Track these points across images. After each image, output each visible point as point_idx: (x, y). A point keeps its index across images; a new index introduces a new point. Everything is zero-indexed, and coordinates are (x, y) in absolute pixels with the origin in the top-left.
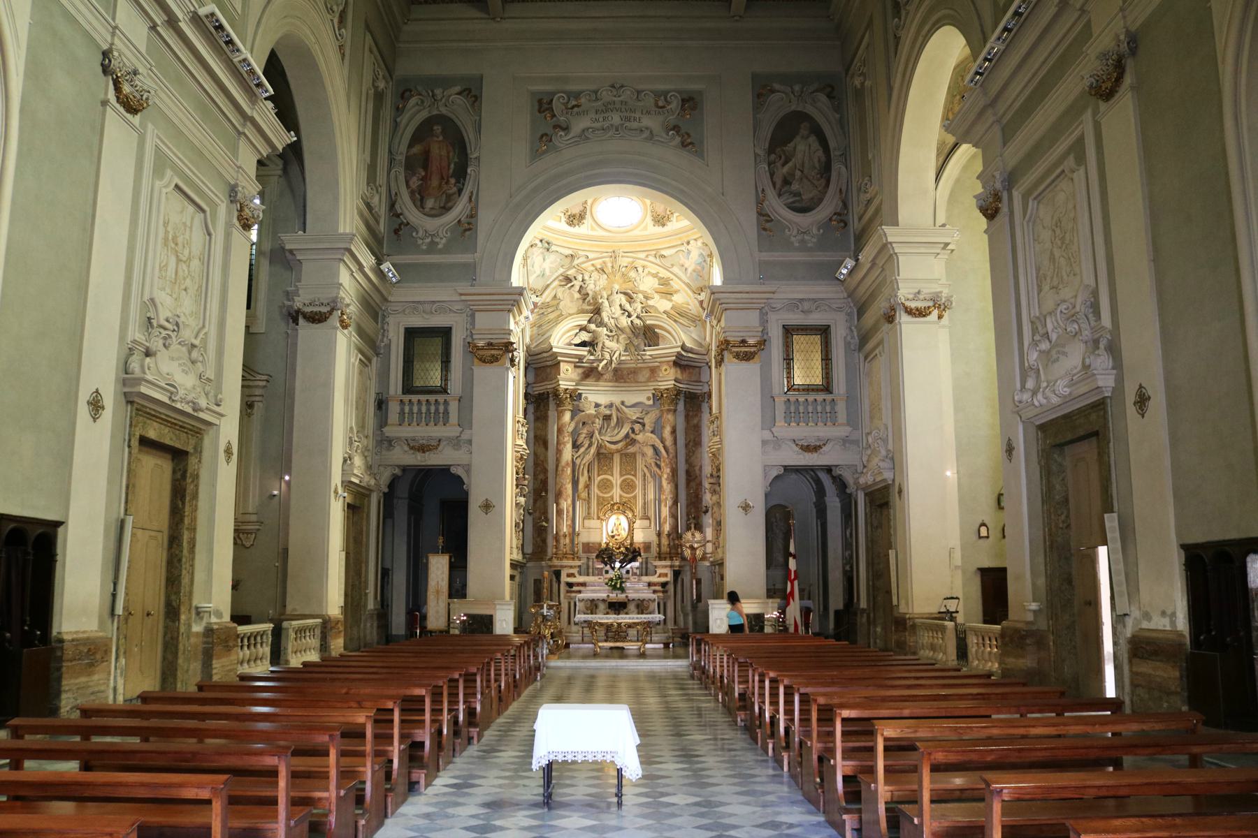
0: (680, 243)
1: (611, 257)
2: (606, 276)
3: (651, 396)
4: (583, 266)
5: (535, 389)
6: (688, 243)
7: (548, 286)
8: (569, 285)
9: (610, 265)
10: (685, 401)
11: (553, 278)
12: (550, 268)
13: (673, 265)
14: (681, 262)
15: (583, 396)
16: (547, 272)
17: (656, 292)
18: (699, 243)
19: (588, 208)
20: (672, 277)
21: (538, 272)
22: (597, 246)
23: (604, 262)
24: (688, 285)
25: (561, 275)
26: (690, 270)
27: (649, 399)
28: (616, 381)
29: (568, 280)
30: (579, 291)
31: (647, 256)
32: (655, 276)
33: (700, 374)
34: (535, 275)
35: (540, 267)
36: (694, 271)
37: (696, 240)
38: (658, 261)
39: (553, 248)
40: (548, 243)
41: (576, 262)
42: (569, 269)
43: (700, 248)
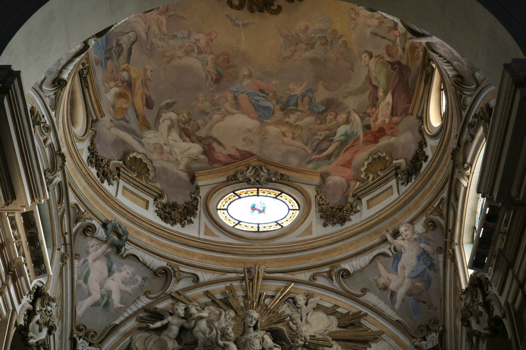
0: (377, 240)
1: (243, 279)
2: (232, 314)
4: (189, 294)
6: (396, 234)
7: (116, 327)
8: (158, 324)
9: (240, 293)
11: (126, 315)
12: (122, 292)
13: (364, 291)
14: (382, 281)
16: (116, 298)
17: (333, 340)
18: (419, 227)
19: (201, 201)
20: (364, 310)
21: (96, 296)
22: (217, 260)
23: (231, 289)
24: (397, 324)
25: (145, 309)
26: (401, 293)
29: (158, 316)
30: (178, 339)
31: (313, 278)
32: (331, 312)
34: (89, 301)
35: (102, 286)
36: (409, 293)
37: (412, 222)
38: (336, 285)
39: (129, 249)
40: (119, 236)
41: (175, 287)
42: (159, 299)
43: (418, 240)
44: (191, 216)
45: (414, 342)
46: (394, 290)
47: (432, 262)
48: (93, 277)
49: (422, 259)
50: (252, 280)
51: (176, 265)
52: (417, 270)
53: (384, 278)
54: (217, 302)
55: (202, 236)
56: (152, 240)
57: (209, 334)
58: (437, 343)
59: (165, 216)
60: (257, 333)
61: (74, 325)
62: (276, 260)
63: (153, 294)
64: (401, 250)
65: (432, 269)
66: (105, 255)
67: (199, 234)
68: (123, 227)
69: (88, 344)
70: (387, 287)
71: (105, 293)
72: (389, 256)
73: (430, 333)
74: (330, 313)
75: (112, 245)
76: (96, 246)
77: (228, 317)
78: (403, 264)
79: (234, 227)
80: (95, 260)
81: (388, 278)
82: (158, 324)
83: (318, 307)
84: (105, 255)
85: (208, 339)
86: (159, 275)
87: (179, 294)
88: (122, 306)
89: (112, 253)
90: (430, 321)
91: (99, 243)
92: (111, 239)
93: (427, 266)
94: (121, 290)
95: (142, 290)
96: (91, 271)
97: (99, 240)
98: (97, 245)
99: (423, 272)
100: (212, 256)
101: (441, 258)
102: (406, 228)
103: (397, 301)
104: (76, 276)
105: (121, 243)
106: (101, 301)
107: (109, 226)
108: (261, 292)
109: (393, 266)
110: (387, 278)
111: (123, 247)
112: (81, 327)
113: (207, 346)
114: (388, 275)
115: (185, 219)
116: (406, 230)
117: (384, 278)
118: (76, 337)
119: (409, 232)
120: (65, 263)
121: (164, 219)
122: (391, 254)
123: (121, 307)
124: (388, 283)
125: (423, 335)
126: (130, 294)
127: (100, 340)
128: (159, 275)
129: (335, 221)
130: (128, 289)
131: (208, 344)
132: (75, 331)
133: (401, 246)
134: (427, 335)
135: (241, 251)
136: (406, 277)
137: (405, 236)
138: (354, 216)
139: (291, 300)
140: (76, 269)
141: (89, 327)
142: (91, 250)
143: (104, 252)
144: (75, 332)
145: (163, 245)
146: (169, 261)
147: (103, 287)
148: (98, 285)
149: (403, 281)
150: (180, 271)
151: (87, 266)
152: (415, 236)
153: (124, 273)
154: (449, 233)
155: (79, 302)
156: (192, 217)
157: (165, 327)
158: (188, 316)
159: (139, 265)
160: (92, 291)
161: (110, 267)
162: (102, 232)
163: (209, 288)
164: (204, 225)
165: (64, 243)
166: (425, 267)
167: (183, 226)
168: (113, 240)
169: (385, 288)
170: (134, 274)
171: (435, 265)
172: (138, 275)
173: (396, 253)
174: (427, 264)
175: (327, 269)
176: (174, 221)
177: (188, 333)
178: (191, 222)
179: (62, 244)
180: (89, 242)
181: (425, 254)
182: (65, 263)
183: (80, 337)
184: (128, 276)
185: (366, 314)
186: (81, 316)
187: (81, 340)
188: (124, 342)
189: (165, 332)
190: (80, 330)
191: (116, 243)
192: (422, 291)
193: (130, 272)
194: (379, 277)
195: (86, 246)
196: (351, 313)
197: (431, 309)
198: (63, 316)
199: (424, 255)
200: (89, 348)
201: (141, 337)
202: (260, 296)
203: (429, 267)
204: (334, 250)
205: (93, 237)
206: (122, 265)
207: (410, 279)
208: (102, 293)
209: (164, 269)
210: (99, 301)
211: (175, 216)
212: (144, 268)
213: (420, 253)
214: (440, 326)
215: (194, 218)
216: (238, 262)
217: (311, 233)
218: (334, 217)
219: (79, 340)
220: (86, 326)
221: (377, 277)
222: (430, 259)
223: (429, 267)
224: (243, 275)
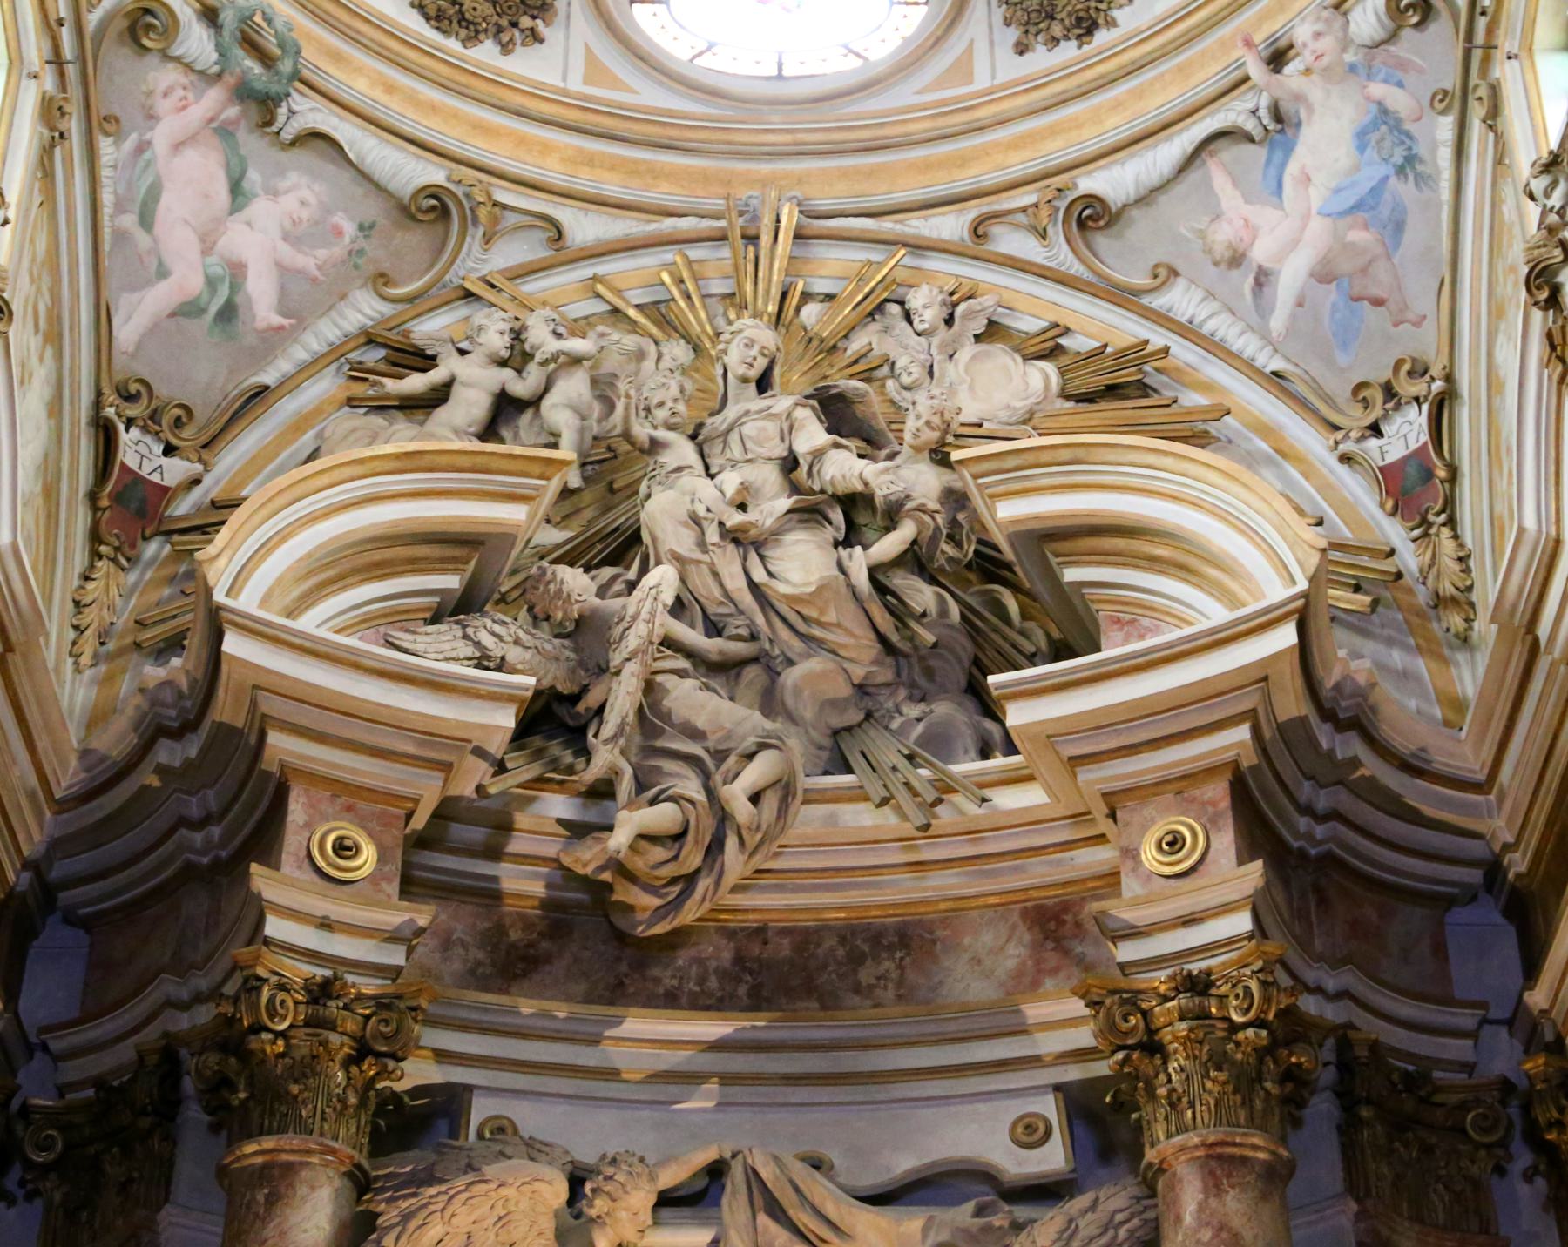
2: (678, 351)
3: (1048, 1107)
5: (73, 1071)
10: (1348, 1129)
12: (283, 269)
14: (1223, 235)
15: (481, 1110)
20: (1158, 338)
21: (187, 279)
25: (370, 339)
26: (1291, 278)
27: (1030, 1134)
28: (757, 1002)
31: (978, 231)
33: (1439, 949)
36: (1324, 274)
44: (534, 17)
45: (1337, 443)
46: (1267, 265)
47: (1410, 149)
48: (174, 207)
49: (1373, 143)
50: (752, 239)
51: (480, 182)
52: (1353, 185)
53: (1230, 222)
54: (632, 313)
55: (576, 84)
56: (390, 89)
57: (599, 421)
58: (1425, 437)
59: (439, 10)
60: (767, 402)
61: (104, 376)
62: (844, 173)
63: (396, 285)
64: (1297, 112)
65: (1411, 177)
66: (215, 130)
67: (564, 79)
68: (279, 23)
69: (162, 448)
70: (1243, 256)
71: (219, 270)
72: (1252, 140)
73: (1398, 407)
74: (1033, 349)
75: (244, 93)
76: (181, 93)
77: (666, 363)
78: (1303, 167)
79: (691, 60)
80: (178, 147)
81: (1246, 221)
82: (416, 383)
83: (993, 331)
84: (215, 130)
85: (595, 438)
86: (421, 217)
87: (493, 286)
88: (286, 322)
89: (243, 122)
90: (1398, 365)
91: (192, 82)
92: (238, 70)
93: (1390, 167)
94: (279, 265)
95: (356, 267)
96: (167, 185)
97: (193, 71)
98: (185, 88)
99: (1377, 191)
100: (612, 156)
101: (1445, 127)
102: (1319, 27)
103: (1279, 304)
104: (107, 198)
105: (275, 88)
106: (205, 297)
107: (228, 18)
108: (787, 283)
109: (1265, 175)
110: (1242, 222)
111: (281, 101)
112: (133, 388)
113: (591, 463)
114: (1247, 210)
115: (514, 25)
116: (1318, 35)
117: (1230, 222)
118: (116, 419)
119: (1327, 43)
120: (62, 135)
121: (438, 18)
122: (1257, 133)
123: (281, 328)
124: (1246, 239)
125: (1369, 421)
126: (314, 280)
127: (204, 439)
128: (421, 217)
129: (1057, 30)
130: (307, 261)
131: (597, 454)
132: (110, 397)
133: (1299, 98)
134: (1386, 416)
135: (719, 142)
136: (1314, 211)
137: (1313, 58)
138: (1127, 9)
139: (894, 309)
140: (105, 173)
141: (162, 390)
142: (163, 106)
143: (212, 120)
144: (111, 398)
145: (434, 109)
146: (453, 165)
147: (212, 248)
148: (192, 238)
149: (1304, 227)
150: (496, 204)
151: (148, 164)
152: (1349, 57)
153: (289, 203)
154: (1481, 23)
155: (125, 295)
156: (539, 22)
157: (439, 396)
158: (517, 356)
159: (346, 176)
160: (167, 259)
161: (237, 175)
162: (201, 39)
163: (604, 268)
164: (581, 51)
165: (52, 58)
166: (1385, 170)
167: (506, 49)
168: (243, 72)
169: (1236, 259)
170: (327, 211)
171: (1421, 161)
172: (340, 214)
173: (1279, 127)
174: (1393, 160)
175: (1026, 197)
176: (472, 27)
177: (528, 415)
178: (535, 37)
179: (47, 62)
180: (151, 75)
181: (1385, 123)
182: (62, 135)
183: (130, 423)
184: (305, 214)
185: (1166, 351)
186: (131, 349)
187: (135, 433)
188: (293, 448)
189: (441, 413)
190: (130, 398)
191: (258, 85)
192: (1370, 263)
193: (312, 199)
194: (1213, 221)
195: (144, 88)
196: (1109, 350)
197: (1402, 323)
198: (60, 336)
199: (1384, 128)
200: (165, 461)
201: (354, 430)
202: (784, 295)
203: (1400, 171)
204: (1053, 131)
205: (166, 57)
206: (282, 172)
207: (1328, 221)
208: (211, 270)
209: (433, 192)
210: (199, 297)
211: (475, 9)
212: (358, 190)
213: (1367, 119)
214: (1433, 379)
215: (547, 23)
216: (705, 178)
217: (969, 78)
218: (1053, 18)
219: (127, 430)
220: (154, 386)
221: (1207, 219)
222: (1404, 138)
223: (1400, 171)
224: (723, 223)
